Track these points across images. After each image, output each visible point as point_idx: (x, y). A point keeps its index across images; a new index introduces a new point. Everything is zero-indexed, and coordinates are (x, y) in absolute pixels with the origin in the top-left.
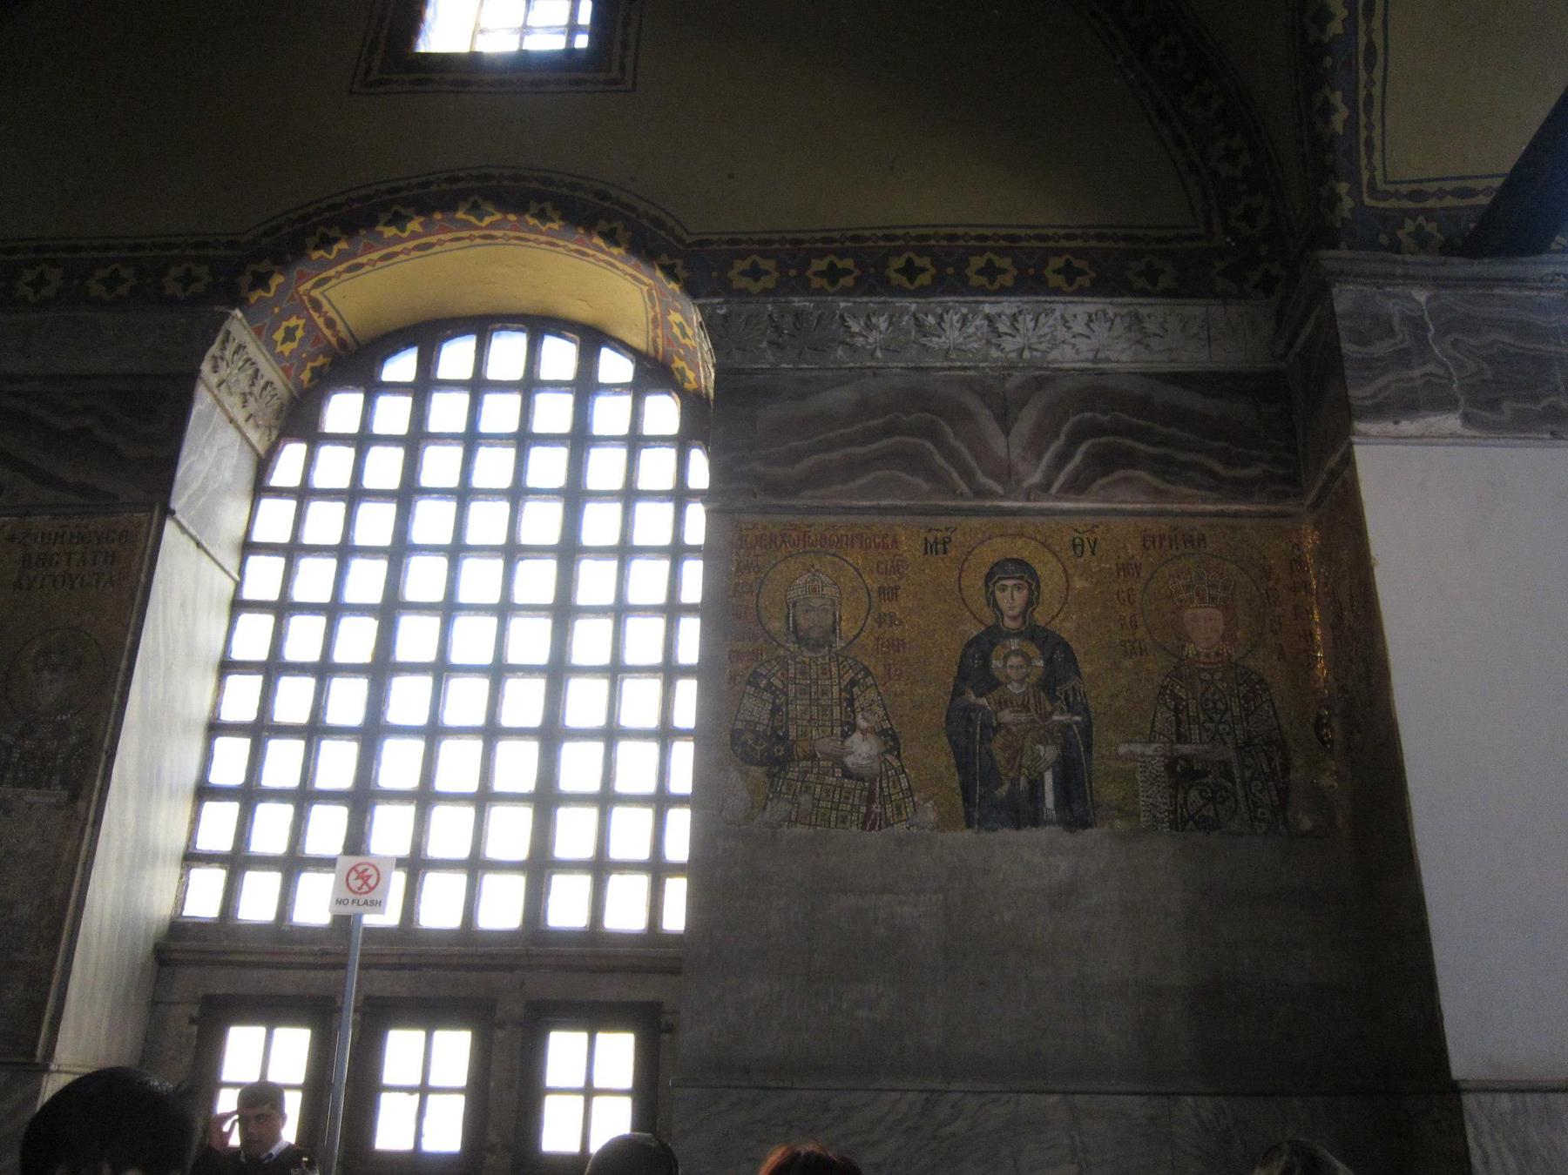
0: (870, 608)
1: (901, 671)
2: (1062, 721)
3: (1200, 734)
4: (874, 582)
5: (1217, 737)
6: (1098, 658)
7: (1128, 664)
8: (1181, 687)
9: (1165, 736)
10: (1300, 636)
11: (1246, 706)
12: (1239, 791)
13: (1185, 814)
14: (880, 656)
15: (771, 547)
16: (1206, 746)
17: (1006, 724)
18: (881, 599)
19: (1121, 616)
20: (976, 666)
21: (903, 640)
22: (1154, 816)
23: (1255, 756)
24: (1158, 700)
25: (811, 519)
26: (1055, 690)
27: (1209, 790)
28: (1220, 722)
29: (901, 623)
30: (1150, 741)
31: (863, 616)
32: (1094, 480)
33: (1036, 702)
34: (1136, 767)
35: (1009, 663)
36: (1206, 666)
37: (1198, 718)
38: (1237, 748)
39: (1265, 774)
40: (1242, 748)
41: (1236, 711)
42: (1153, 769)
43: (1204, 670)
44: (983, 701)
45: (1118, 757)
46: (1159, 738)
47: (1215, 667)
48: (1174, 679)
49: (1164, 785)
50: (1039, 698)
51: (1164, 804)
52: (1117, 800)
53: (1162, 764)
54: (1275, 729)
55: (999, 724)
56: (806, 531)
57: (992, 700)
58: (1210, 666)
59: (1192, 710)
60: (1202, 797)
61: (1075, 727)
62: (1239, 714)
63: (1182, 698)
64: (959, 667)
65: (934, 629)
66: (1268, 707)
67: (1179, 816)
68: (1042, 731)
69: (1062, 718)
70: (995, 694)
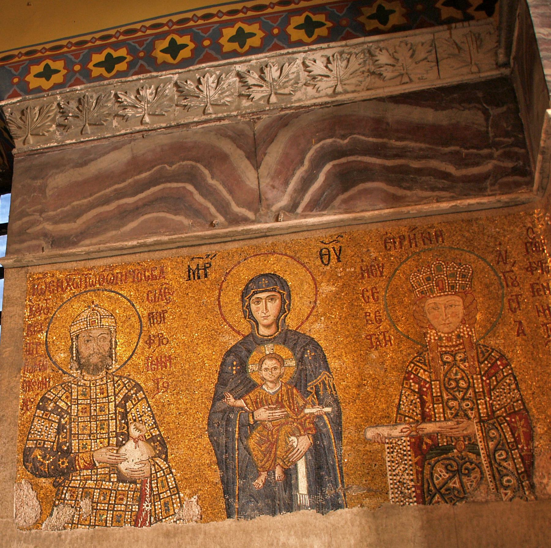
0: (141, 333)
1: (168, 383)
2: (313, 413)
3: (444, 413)
4: (145, 310)
5: (461, 413)
6: (346, 353)
7: (374, 355)
8: (425, 371)
9: (410, 417)
10: (538, 311)
11: (488, 381)
12: (483, 462)
13: (432, 488)
14: (150, 372)
15: (58, 291)
16: (449, 423)
17: (262, 421)
18: (151, 323)
19: (366, 313)
20: (234, 372)
21: (171, 355)
22: (401, 493)
23: (499, 428)
24: (402, 386)
25: (91, 263)
26: (306, 386)
27: (454, 464)
28: (463, 399)
29: (168, 342)
30: (396, 424)
31: (136, 340)
32: (337, 195)
33: (288, 398)
34: (384, 449)
35: (264, 366)
36: (448, 349)
37: (441, 396)
38: (481, 421)
39: (508, 443)
40: (483, 421)
41: (479, 387)
42: (400, 449)
43: (446, 353)
44: (241, 403)
45: (366, 441)
46: (405, 420)
47: (457, 348)
48: (418, 364)
49: (410, 463)
50: (292, 393)
51: (412, 480)
52: (366, 481)
53: (409, 443)
54: (517, 401)
55: (255, 422)
56: (86, 275)
57: (249, 401)
58: (452, 349)
59: (436, 391)
60: (448, 471)
61: (325, 418)
62: (481, 390)
63: (425, 380)
64: (219, 374)
65: (197, 344)
66: (510, 380)
67: (425, 490)
68: (295, 424)
69: (314, 410)
70: (252, 396)
